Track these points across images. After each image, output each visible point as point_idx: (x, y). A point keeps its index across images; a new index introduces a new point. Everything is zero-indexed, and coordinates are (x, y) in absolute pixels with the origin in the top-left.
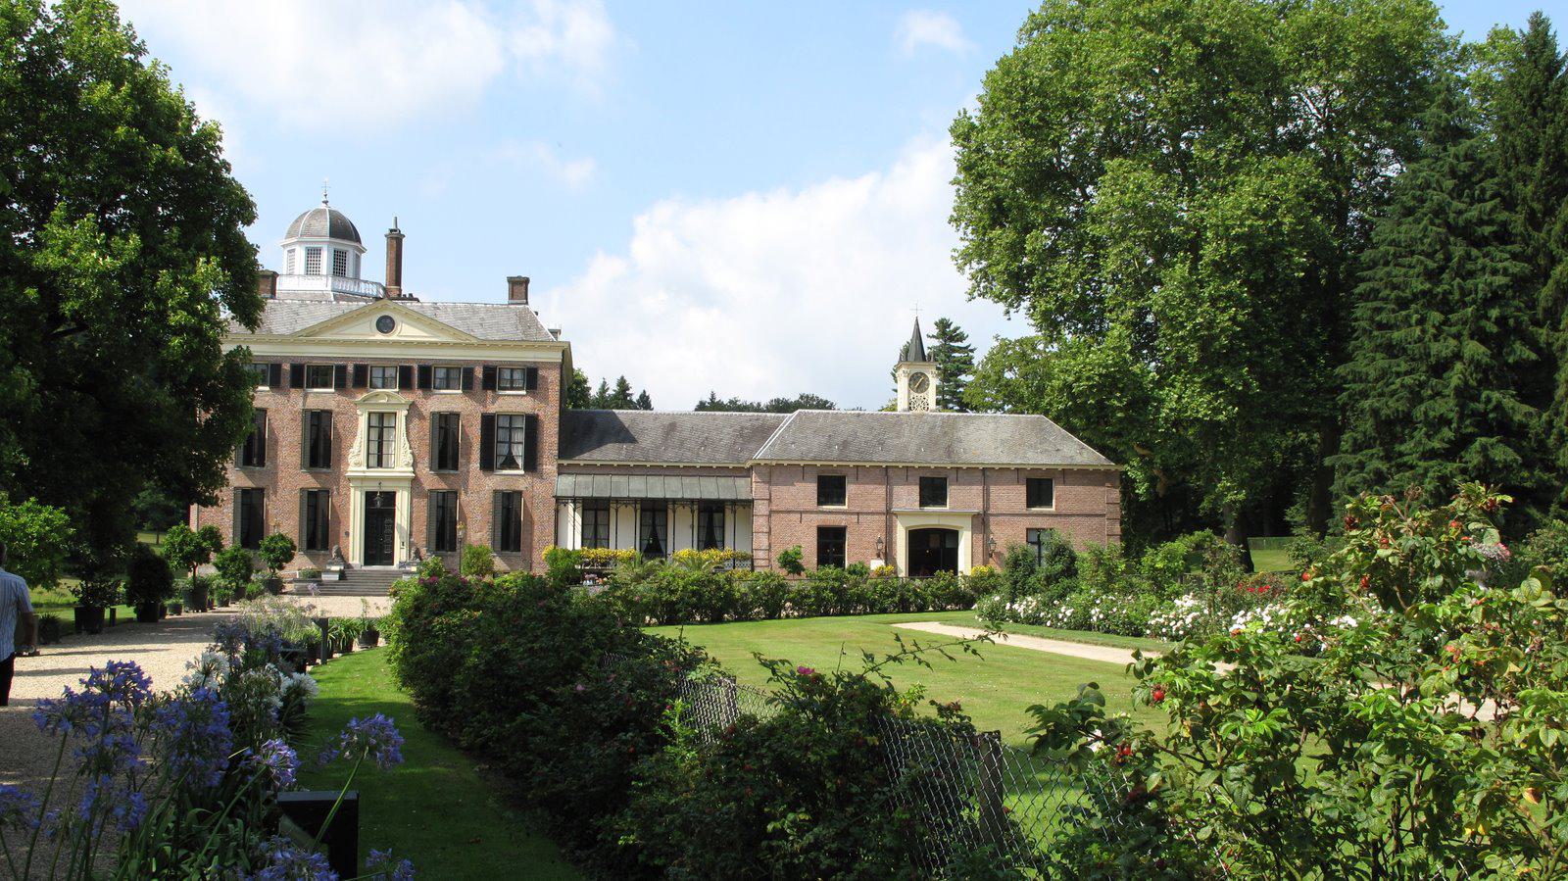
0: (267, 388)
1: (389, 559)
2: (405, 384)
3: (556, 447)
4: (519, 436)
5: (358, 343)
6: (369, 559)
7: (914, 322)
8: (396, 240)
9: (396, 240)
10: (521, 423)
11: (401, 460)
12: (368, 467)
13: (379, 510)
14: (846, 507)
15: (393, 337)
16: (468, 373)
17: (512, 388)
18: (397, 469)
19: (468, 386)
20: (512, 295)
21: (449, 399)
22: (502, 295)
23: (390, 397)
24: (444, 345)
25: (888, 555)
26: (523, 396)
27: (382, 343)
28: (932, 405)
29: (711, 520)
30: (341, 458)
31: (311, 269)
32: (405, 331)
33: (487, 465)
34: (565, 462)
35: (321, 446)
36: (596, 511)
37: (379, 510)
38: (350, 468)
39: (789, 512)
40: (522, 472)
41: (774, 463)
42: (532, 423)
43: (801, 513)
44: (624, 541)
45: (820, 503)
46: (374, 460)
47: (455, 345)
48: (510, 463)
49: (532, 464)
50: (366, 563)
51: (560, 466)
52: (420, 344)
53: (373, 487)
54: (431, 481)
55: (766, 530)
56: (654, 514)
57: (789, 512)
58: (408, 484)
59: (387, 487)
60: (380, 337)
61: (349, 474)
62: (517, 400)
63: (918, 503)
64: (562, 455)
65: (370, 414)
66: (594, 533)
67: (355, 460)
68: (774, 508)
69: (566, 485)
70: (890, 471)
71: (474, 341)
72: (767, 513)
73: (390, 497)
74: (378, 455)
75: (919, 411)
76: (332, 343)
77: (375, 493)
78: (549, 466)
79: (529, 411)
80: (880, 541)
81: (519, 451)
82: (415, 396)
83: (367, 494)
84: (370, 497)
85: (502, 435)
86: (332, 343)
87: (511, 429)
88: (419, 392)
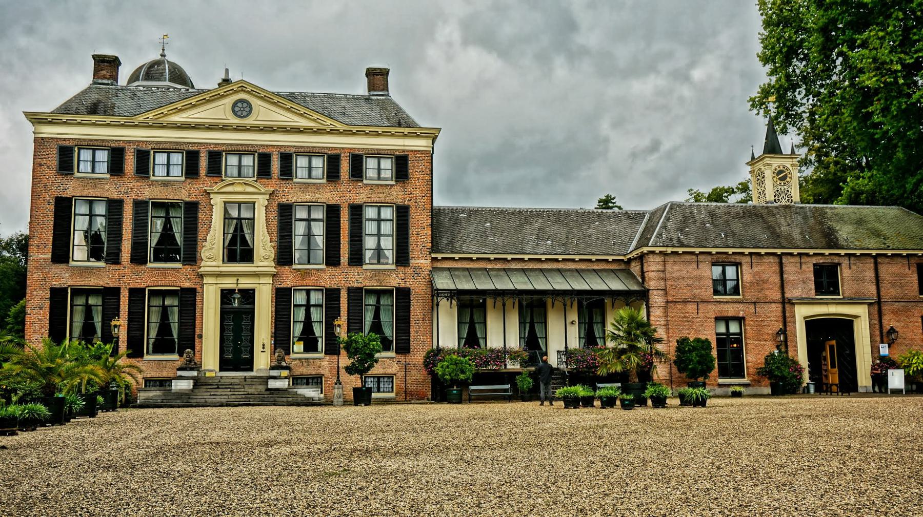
0: (108, 176)
1: (248, 365)
4: (388, 228)
5: (211, 127)
6: (224, 365)
10: (387, 213)
14: (741, 297)
15: (250, 121)
16: (333, 161)
17: (379, 178)
20: (371, 87)
22: (361, 88)
26: (392, 186)
28: (796, 197)
32: (263, 113)
34: (439, 256)
38: (203, 264)
39: (685, 302)
40: (393, 267)
41: (669, 250)
47: (318, 132)
50: (221, 370)
51: (434, 260)
53: (229, 283)
57: (685, 302)
58: (269, 280)
59: (246, 283)
60: (236, 121)
61: (202, 269)
62: (387, 191)
63: (813, 292)
65: (225, 203)
68: (671, 299)
70: (784, 260)
72: (663, 304)
73: (248, 295)
75: (784, 203)
77: (232, 291)
78: (421, 260)
79: (400, 202)
81: (388, 244)
83: (222, 290)
84: (226, 295)
85: (370, 228)
87: (379, 220)
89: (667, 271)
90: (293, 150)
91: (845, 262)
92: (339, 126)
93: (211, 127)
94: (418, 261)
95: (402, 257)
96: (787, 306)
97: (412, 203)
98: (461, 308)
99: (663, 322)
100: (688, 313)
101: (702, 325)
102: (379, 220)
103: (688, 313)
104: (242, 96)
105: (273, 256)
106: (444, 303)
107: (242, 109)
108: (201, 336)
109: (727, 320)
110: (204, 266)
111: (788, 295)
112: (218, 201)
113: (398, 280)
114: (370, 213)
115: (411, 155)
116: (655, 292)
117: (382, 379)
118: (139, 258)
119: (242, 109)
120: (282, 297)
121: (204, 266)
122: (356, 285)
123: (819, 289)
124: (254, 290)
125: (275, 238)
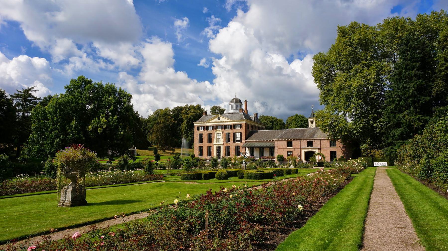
2: (222, 129)
4: (239, 136)
5: (215, 122)
7: (312, 111)
8: (246, 102)
9: (246, 102)
10: (239, 134)
11: (221, 141)
13: (219, 149)
16: (231, 126)
19: (231, 128)
21: (228, 130)
23: (220, 131)
24: (227, 122)
25: (300, 156)
27: (218, 122)
29: (272, 150)
30: (213, 141)
31: (232, 108)
33: (235, 141)
35: (210, 140)
36: (252, 150)
37: (219, 149)
42: (241, 134)
44: (257, 153)
45: (288, 146)
47: (229, 122)
48: (238, 141)
49: (240, 141)
51: (246, 141)
52: (224, 122)
53: (218, 146)
54: (226, 144)
56: (262, 150)
59: (219, 146)
60: (218, 121)
63: (306, 146)
64: (246, 139)
66: (252, 153)
67: (215, 142)
68: (279, 148)
73: (220, 147)
74: (218, 140)
75: (312, 127)
76: (213, 122)
78: (244, 141)
79: (240, 132)
80: (298, 154)
81: (239, 139)
86: (212, 122)
87: (238, 135)
91: (313, 141)
92: (232, 120)
93: (215, 122)
96: (301, 149)
97: (242, 132)
98: (250, 149)
99: (277, 152)
102: (238, 135)
104: (219, 117)
106: (247, 149)
107: (219, 119)
109: (290, 152)
111: (301, 147)
112: (216, 133)
114: (237, 134)
119: (219, 119)
123: (308, 146)
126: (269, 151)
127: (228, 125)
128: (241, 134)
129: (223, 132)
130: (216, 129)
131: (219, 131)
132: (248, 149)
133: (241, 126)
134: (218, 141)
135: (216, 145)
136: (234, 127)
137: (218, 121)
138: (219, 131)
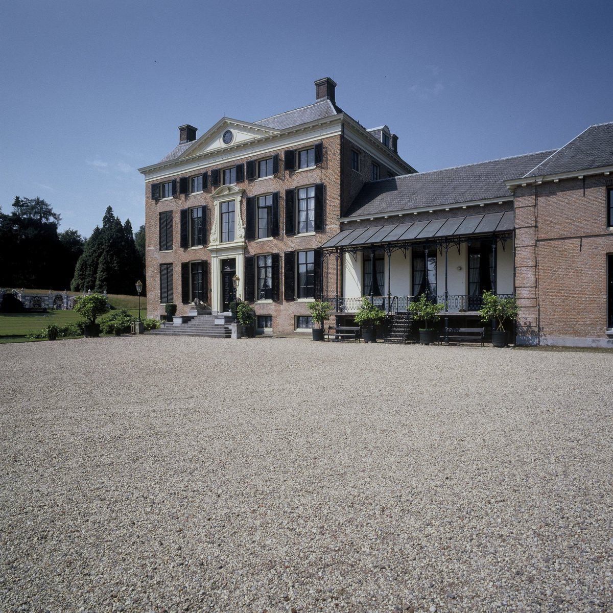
2: (239, 179)
3: (338, 208)
12: (221, 241)
18: (235, 241)
19: (276, 171)
32: (240, 137)
34: (346, 220)
38: (211, 244)
42: (320, 190)
43: (581, 237)
46: (225, 236)
51: (342, 224)
53: (225, 256)
55: (530, 263)
59: (230, 255)
62: (310, 174)
68: (543, 236)
69: (347, 238)
71: (272, 133)
72: (532, 243)
73: (231, 263)
78: (332, 224)
79: (318, 182)
82: (245, 185)
85: (303, 205)
88: (247, 182)
89: (539, 206)
90: (254, 158)
94: (330, 226)
95: (320, 225)
97: (326, 183)
98: (365, 260)
99: (531, 263)
100: (566, 250)
101: (586, 264)
103: (566, 250)
105: (244, 235)
108: (211, 290)
110: (211, 246)
113: (316, 243)
114: (303, 195)
115: (326, 144)
116: (522, 231)
117: (301, 318)
118: (185, 244)
119: (228, 137)
120: (250, 263)
121: (211, 246)
122: (291, 249)
124: (235, 259)
125: (245, 223)
126: (464, 264)
127: (265, 159)
128: (320, 190)
129: (244, 193)
130: (216, 183)
131: (227, 192)
132: (355, 260)
133: (319, 153)
134: (225, 236)
135: (217, 251)
136: (291, 161)
137: (224, 146)
138: (227, 192)
